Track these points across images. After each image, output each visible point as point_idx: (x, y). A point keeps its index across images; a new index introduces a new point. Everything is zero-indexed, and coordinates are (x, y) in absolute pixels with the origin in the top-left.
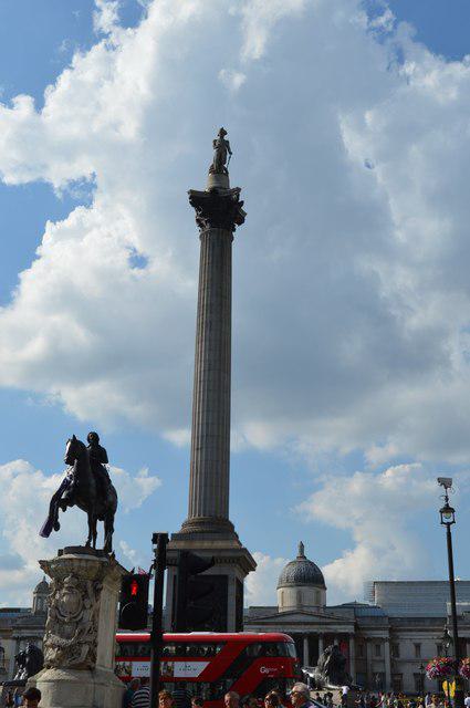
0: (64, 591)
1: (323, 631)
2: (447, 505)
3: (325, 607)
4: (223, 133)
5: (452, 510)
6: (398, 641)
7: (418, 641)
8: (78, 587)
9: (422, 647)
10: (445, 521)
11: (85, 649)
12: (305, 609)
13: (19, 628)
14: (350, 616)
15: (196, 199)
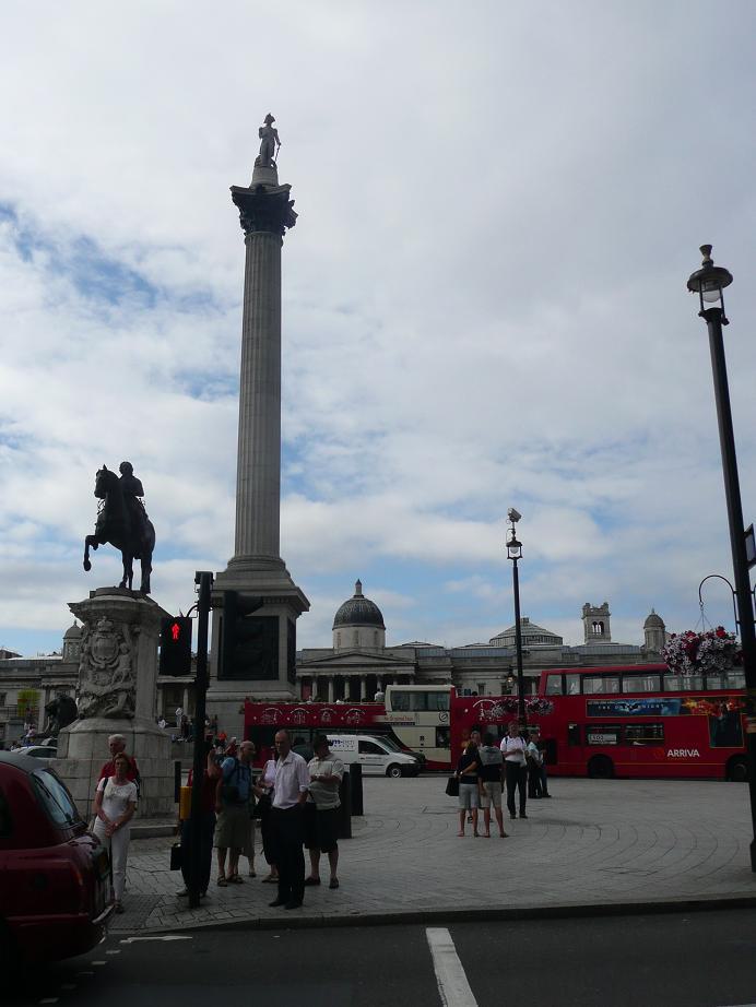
0: (97, 635)
1: (382, 673)
2: (514, 538)
3: (384, 648)
4: (270, 119)
5: (520, 544)
6: (460, 682)
7: (481, 682)
8: (112, 631)
9: (486, 687)
10: (512, 555)
11: (122, 697)
12: (362, 650)
13: (49, 677)
14: (411, 656)
15: (239, 196)
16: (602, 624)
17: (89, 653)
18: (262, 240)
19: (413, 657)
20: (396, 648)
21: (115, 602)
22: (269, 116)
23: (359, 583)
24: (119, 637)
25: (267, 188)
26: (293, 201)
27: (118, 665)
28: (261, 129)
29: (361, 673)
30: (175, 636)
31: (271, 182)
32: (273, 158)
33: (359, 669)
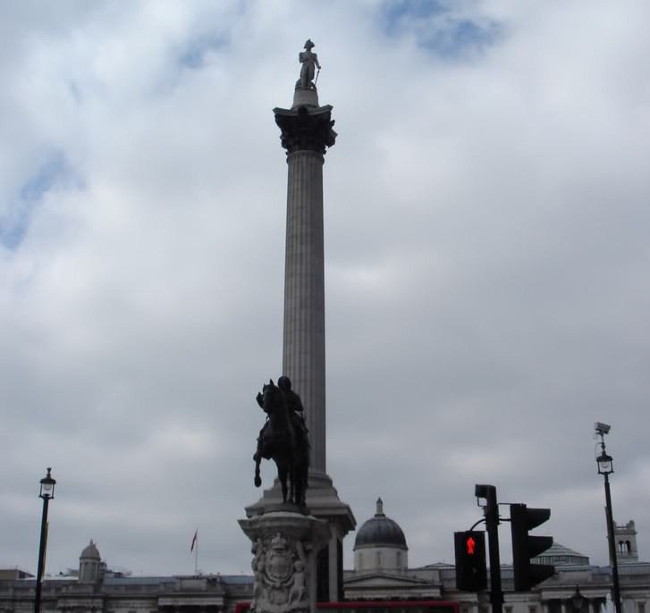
2: (604, 453)
3: (406, 570)
4: (309, 45)
5: (609, 459)
8: (287, 548)
10: (603, 470)
12: (385, 572)
13: (65, 597)
15: (282, 117)
16: (628, 543)
17: (263, 571)
18: (305, 158)
19: (437, 579)
20: (420, 569)
21: (290, 519)
22: (309, 41)
23: (380, 502)
24: (293, 555)
25: (310, 109)
26: (334, 121)
27: (293, 583)
28: (301, 54)
29: (384, 596)
30: (471, 551)
31: (313, 104)
32: (313, 81)
33: (384, 592)
